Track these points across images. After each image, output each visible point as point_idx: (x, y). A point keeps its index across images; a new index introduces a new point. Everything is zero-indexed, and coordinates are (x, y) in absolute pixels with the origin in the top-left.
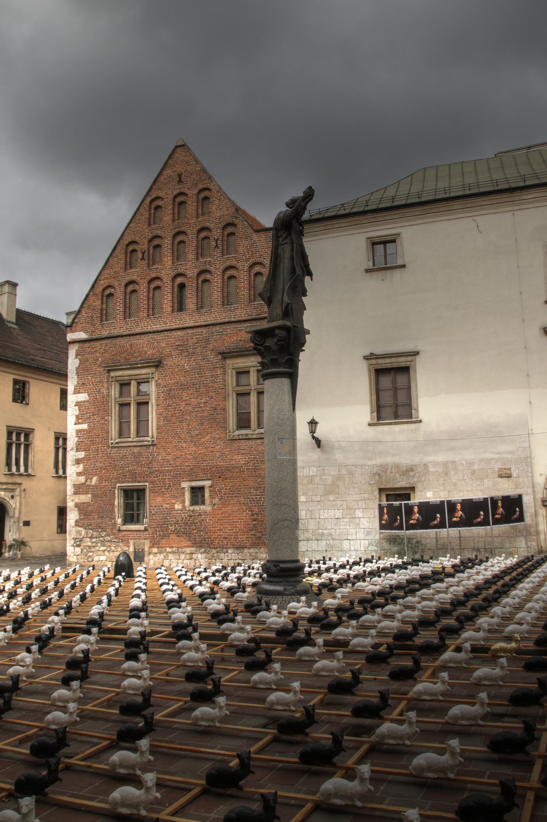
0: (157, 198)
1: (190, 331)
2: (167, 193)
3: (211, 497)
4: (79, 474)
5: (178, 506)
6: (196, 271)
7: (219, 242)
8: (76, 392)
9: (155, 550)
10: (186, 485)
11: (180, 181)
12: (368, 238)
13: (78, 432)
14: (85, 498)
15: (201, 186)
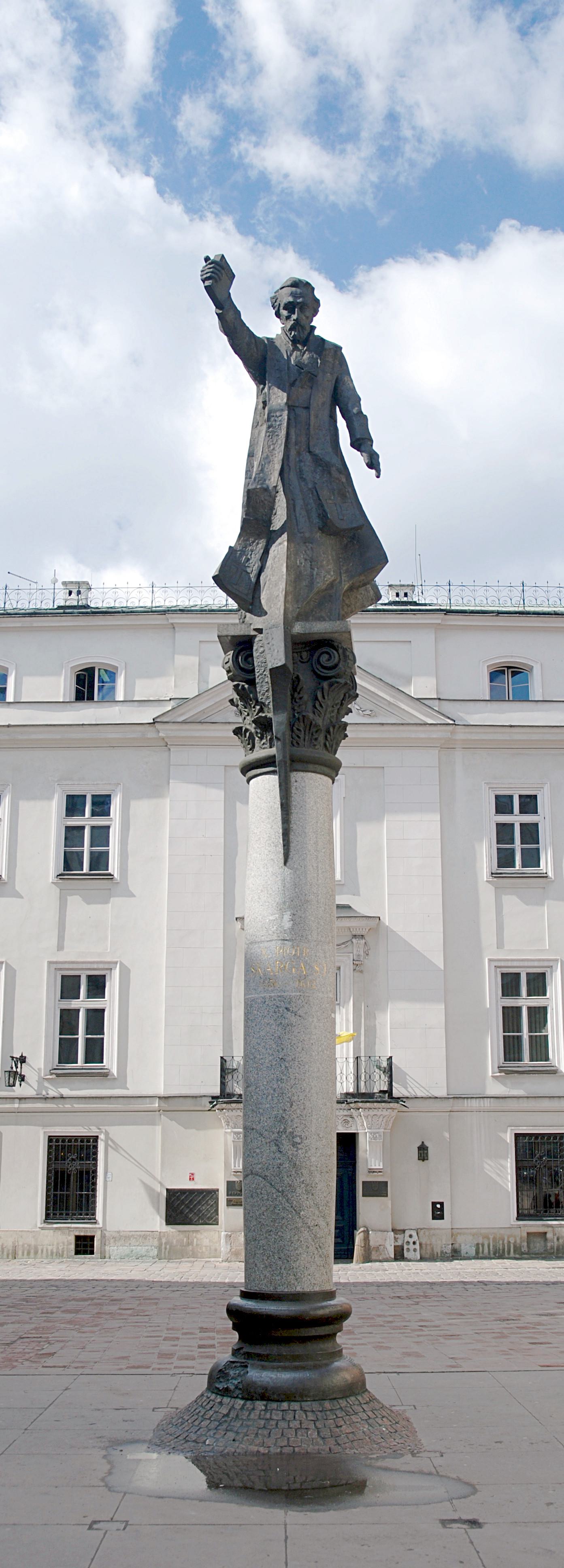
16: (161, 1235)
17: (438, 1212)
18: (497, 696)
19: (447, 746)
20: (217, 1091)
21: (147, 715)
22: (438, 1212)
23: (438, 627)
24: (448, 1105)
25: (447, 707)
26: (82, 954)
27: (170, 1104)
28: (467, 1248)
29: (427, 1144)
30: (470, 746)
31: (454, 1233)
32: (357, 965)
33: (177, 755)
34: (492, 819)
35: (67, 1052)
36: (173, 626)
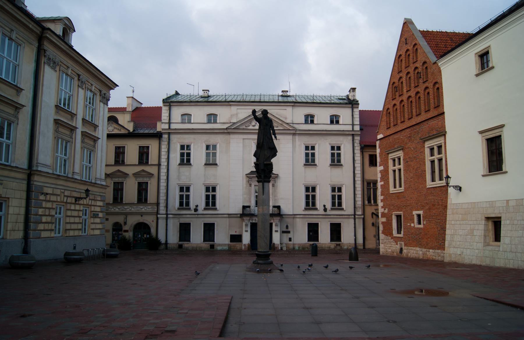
0: (400, 55)
1: (412, 128)
2: (403, 53)
3: (423, 221)
4: (382, 207)
5: (412, 225)
6: (415, 93)
7: (421, 74)
8: (380, 166)
9: (406, 247)
10: (415, 213)
11: (406, 43)
12: (476, 54)
13: (381, 185)
14: (384, 220)
15: (413, 43)
16: (229, 245)
17: (290, 239)
18: (306, 122)
19: (294, 134)
20: (241, 213)
21: (225, 126)
22: (290, 239)
23: (293, 106)
24: (293, 216)
25: (295, 126)
26: (211, 182)
27: (230, 216)
28: (297, 248)
29: (289, 225)
30: (299, 134)
31: (294, 244)
32: (273, 185)
33: (232, 136)
34: (303, 151)
35: (207, 204)
36: (231, 105)
